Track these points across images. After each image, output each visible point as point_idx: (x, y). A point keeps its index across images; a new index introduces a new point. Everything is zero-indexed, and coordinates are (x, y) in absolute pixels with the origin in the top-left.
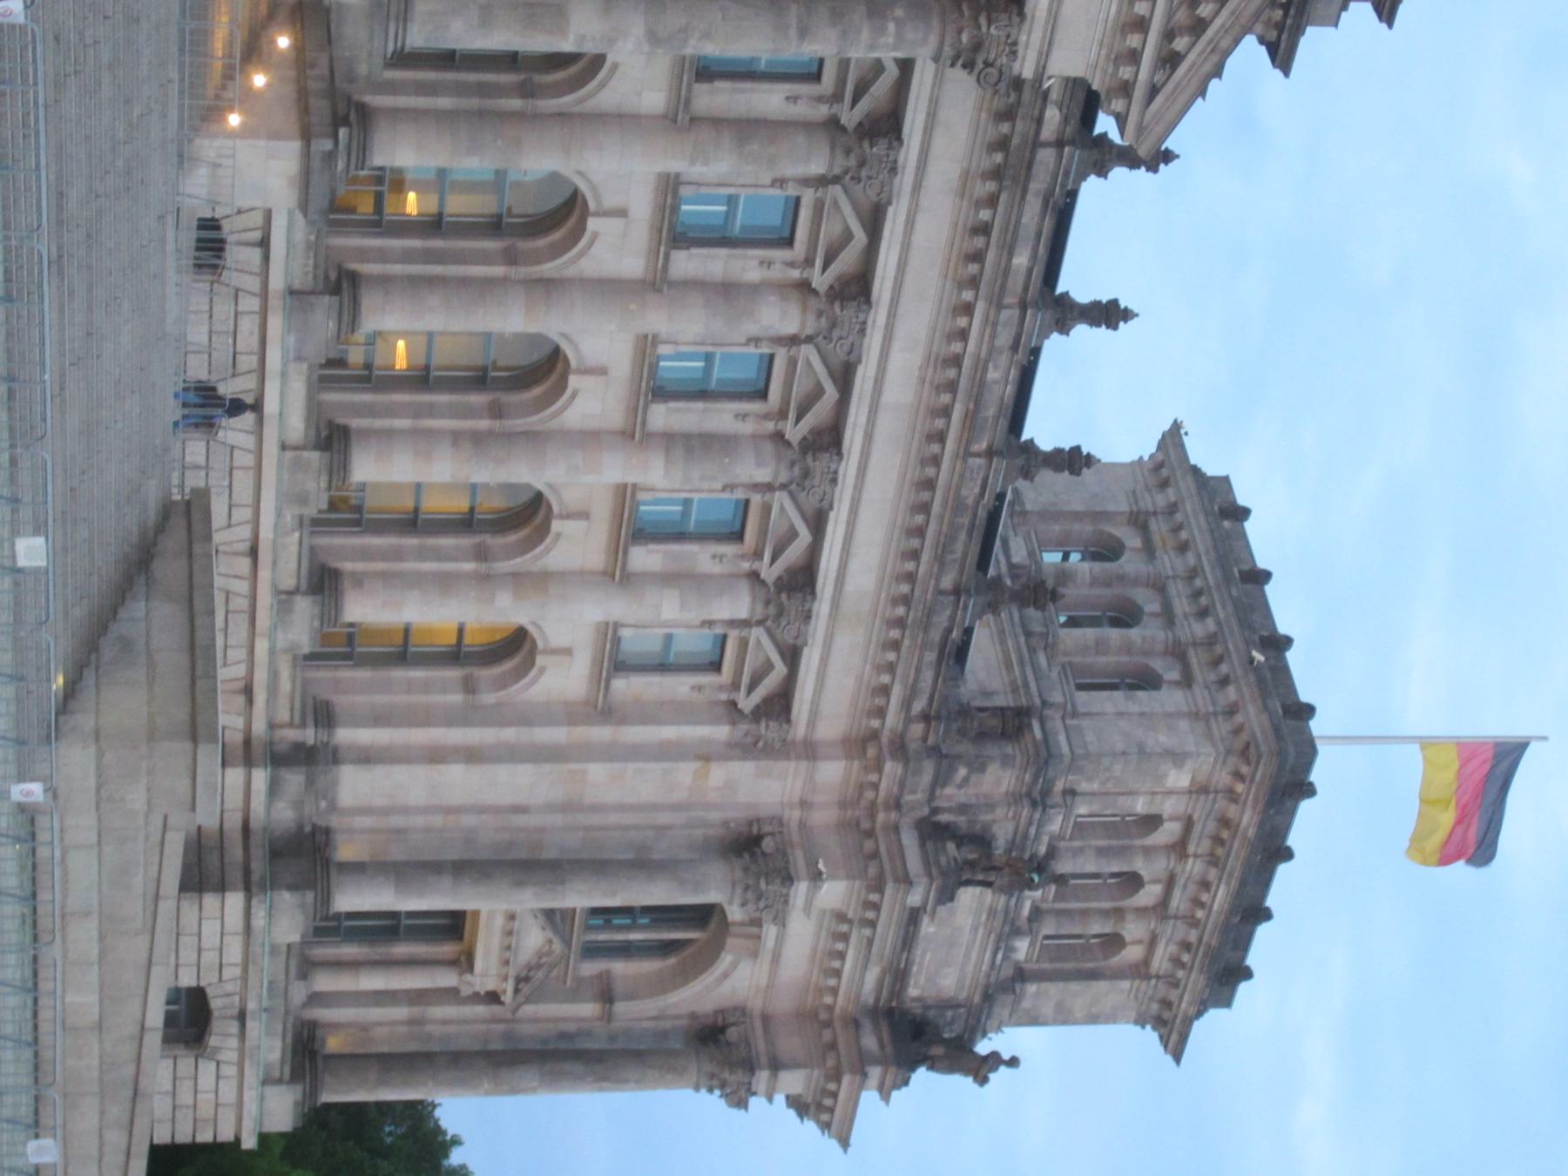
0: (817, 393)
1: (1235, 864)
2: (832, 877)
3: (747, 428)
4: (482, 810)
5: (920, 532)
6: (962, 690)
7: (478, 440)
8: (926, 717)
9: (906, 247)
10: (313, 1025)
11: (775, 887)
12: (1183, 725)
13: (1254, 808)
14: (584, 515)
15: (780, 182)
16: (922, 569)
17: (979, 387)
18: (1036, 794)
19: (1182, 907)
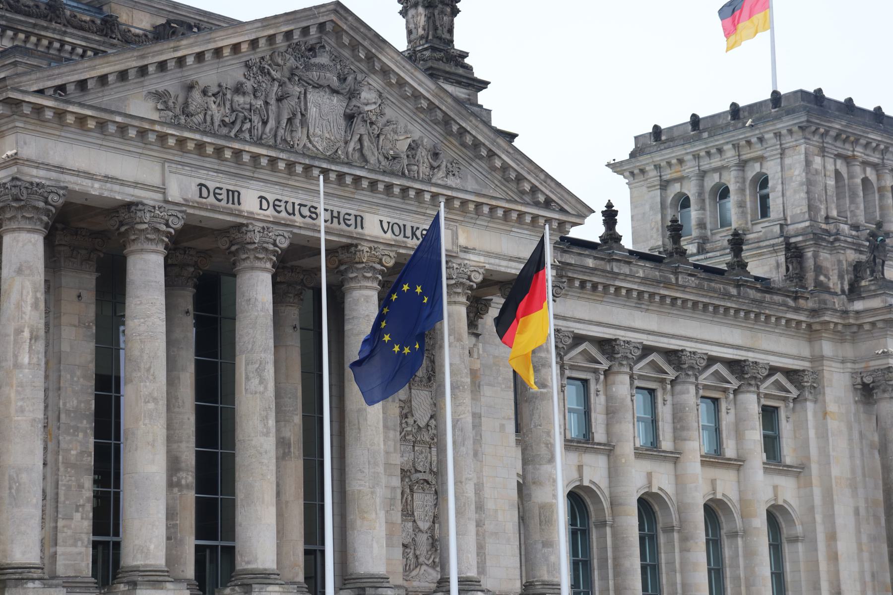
0: (653, 365)
1: (857, 130)
2: (886, 346)
3: (669, 398)
4: (858, 532)
5: (716, 307)
6: (776, 279)
7: (685, 539)
8: (796, 299)
9: (590, 322)
12: (788, 161)
13: (832, 122)
14: (713, 482)
16: (734, 306)
17: (645, 280)
18: (831, 239)
19: (878, 156)
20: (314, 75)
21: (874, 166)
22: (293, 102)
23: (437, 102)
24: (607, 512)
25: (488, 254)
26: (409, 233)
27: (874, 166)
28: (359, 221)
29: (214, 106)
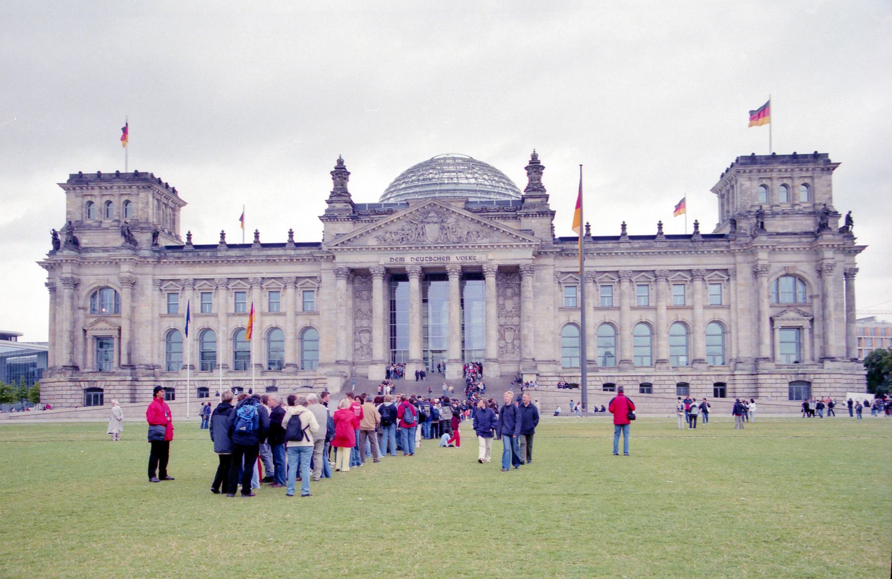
1: (771, 167)
3: (654, 288)
5: (672, 252)
7: (658, 337)
8: (729, 241)
10: (820, 359)
11: (759, 268)
14: (677, 315)
15: (597, 290)
20: (428, 220)
21: (790, 177)
22: (419, 230)
23: (473, 218)
24: (619, 330)
25: (501, 260)
26: (468, 258)
27: (790, 177)
28: (448, 258)
29: (393, 236)
